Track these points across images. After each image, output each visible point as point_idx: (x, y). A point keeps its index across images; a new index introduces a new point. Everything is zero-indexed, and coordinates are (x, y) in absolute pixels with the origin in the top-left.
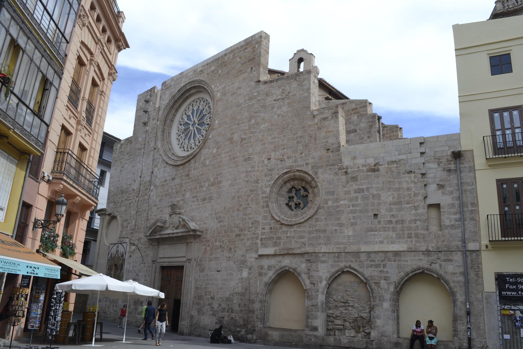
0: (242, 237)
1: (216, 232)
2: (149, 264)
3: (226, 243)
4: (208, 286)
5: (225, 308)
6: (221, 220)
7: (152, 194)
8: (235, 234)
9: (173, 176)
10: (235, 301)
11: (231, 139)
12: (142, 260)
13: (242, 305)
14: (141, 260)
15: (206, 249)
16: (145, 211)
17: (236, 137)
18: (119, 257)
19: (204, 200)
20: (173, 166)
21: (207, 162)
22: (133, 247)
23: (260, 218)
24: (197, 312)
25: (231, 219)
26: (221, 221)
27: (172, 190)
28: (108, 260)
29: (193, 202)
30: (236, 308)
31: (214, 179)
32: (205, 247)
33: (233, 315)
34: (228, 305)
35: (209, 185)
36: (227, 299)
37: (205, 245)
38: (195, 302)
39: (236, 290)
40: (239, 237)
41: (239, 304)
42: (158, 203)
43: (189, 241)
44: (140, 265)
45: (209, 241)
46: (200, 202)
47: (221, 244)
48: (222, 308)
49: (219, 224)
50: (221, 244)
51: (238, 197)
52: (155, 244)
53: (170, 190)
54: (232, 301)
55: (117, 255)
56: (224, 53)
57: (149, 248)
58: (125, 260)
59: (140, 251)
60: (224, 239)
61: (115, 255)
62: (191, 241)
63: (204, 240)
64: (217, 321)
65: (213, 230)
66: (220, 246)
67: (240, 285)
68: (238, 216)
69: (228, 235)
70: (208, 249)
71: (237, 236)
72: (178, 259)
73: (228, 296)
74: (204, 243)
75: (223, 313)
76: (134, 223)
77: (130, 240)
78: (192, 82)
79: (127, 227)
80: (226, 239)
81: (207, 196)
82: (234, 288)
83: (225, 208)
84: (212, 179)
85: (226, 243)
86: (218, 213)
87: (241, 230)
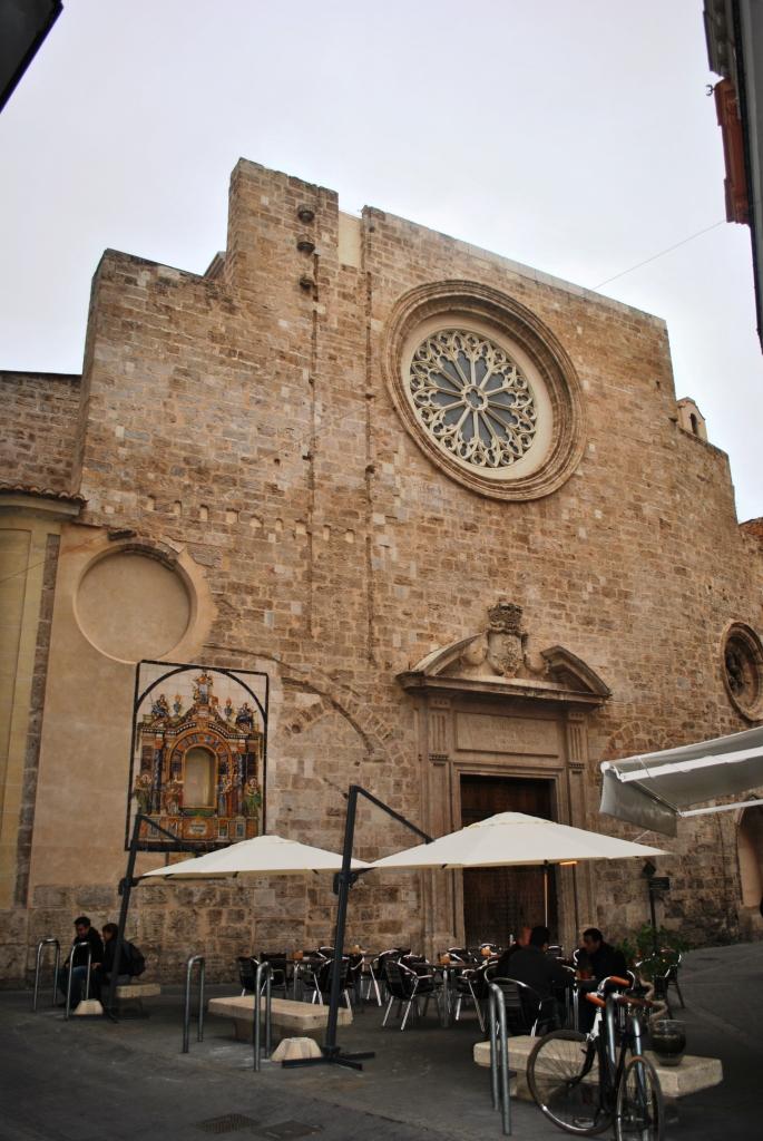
0: (696, 730)
1: (634, 709)
2: (406, 764)
3: (663, 738)
4: (633, 833)
5: (683, 880)
6: (644, 683)
7: (381, 539)
8: (681, 722)
9: (470, 521)
10: (703, 864)
11: (637, 509)
12: (363, 748)
13: (716, 870)
14: (360, 746)
15: (612, 744)
16: (355, 584)
17: (648, 510)
18: (221, 723)
19: (589, 622)
20: (462, 491)
21: (582, 533)
22: (307, 700)
23: (715, 699)
24: (611, 898)
25: (665, 686)
26: (643, 687)
27: (470, 557)
28: (137, 727)
29: (555, 617)
30: (708, 877)
31: (609, 581)
32: (609, 738)
33: (703, 893)
34: (690, 873)
35: (596, 592)
36: (684, 859)
37: (609, 734)
38: (602, 873)
39: (703, 840)
40: (688, 729)
41: (713, 869)
42: (413, 575)
43: (575, 718)
44: (357, 764)
45: (619, 725)
46: (575, 624)
47: (652, 737)
48: (677, 881)
49: (639, 693)
50: (652, 737)
51: (675, 644)
52: (444, 706)
53: (463, 557)
54: (697, 863)
55: (203, 713)
56: (580, 293)
57: (398, 713)
58: (269, 740)
59: (347, 715)
60: (654, 727)
61: (193, 711)
62: (578, 719)
63: (605, 722)
64: (668, 911)
65: (627, 702)
66: (650, 741)
67: (708, 829)
68: (680, 684)
69: (666, 721)
70: (619, 744)
71: (684, 725)
72: (534, 762)
73: (686, 852)
74: (606, 729)
75: (682, 892)
76: (296, 608)
77: (284, 668)
78: (497, 293)
79: (258, 616)
80: (663, 730)
81: (597, 617)
82: (696, 837)
83: (648, 659)
84: (603, 580)
85: (663, 738)
86: (633, 665)
87: (693, 715)
